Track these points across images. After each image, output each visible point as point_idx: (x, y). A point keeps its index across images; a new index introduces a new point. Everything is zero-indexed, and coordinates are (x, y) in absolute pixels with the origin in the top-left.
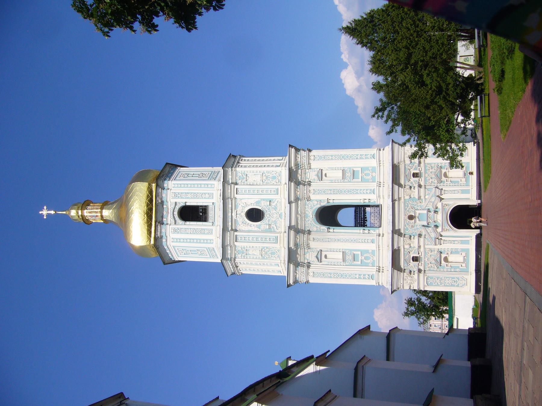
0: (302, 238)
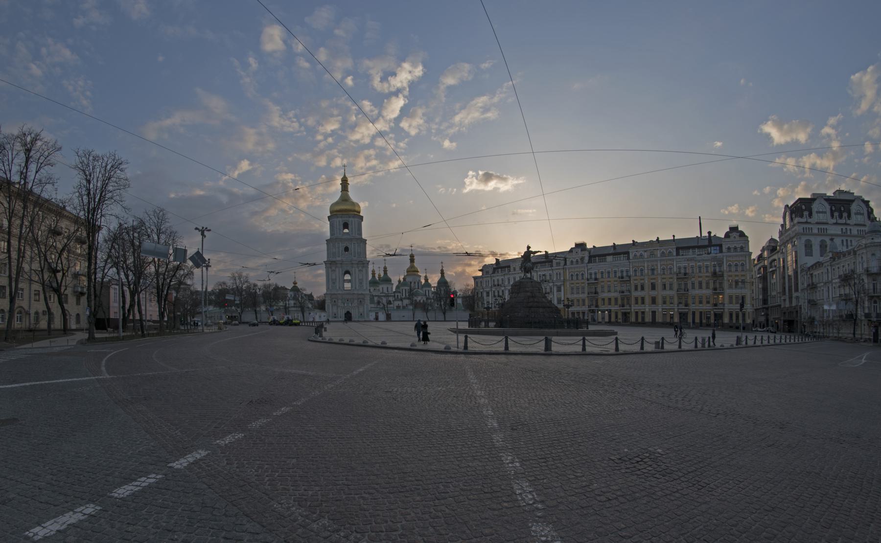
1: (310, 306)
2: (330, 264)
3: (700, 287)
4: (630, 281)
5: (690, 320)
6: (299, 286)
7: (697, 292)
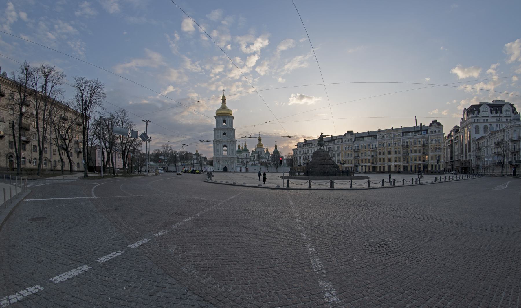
0: (221, 142)
1: (205, 163)
2: (216, 141)
3: (416, 152)
4: (377, 150)
5: (409, 169)
6: (199, 152)
7: (414, 155)
